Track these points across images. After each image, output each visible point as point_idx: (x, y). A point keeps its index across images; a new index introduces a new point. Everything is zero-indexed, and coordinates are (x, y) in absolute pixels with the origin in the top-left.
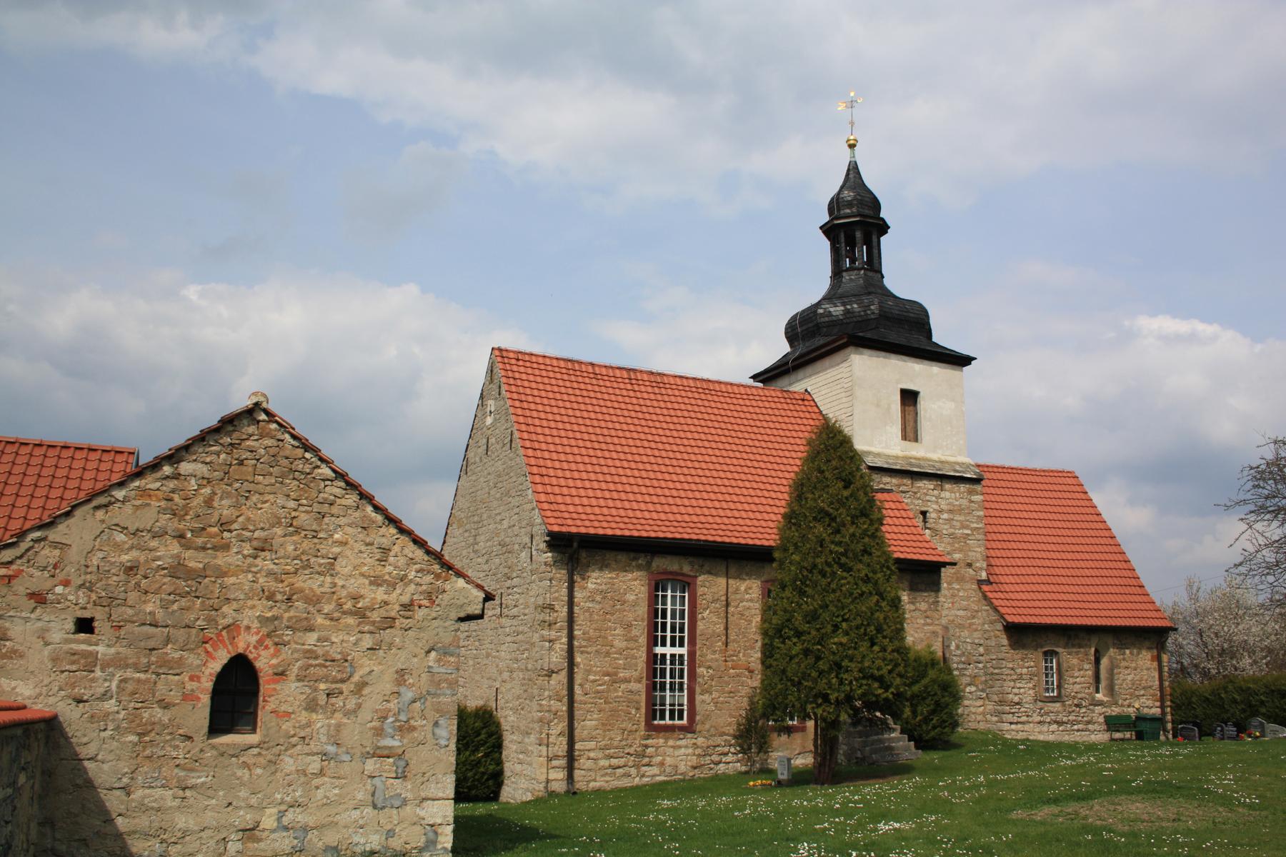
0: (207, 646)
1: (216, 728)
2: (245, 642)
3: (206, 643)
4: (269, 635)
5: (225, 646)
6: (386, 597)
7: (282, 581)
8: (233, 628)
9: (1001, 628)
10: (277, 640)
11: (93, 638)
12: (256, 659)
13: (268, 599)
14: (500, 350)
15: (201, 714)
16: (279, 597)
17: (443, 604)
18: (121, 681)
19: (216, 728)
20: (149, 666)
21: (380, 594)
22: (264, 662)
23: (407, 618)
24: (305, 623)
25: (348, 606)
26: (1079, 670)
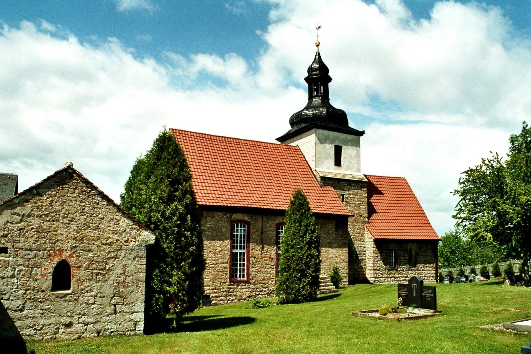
0: (51, 257)
1: (55, 287)
2: (65, 255)
3: (51, 256)
4: (74, 253)
5: (58, 257)
6: (118, 238)
7: (79, 233)
8: (61, 251)
9: (372, 241)
10: (77, 254)
11: (8, 255)
12: (69, 261)
13: (74, 239)
14: (173, 129)
15: (48, 283)
16: (78, 238)
17: (140, 240)
18: (18, 271)
19: (55, 287)
20: (29, 265)
21: (116, 237)
22: (72, 262)
23: (127, 246)
24: (88, 248)
25: (105, 242)
26: (403, 257)
